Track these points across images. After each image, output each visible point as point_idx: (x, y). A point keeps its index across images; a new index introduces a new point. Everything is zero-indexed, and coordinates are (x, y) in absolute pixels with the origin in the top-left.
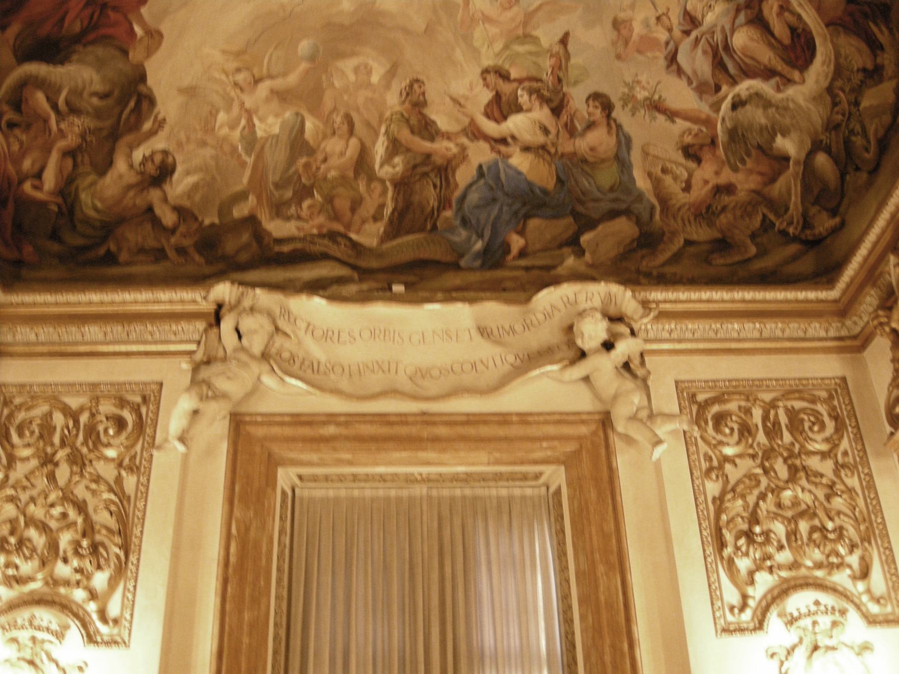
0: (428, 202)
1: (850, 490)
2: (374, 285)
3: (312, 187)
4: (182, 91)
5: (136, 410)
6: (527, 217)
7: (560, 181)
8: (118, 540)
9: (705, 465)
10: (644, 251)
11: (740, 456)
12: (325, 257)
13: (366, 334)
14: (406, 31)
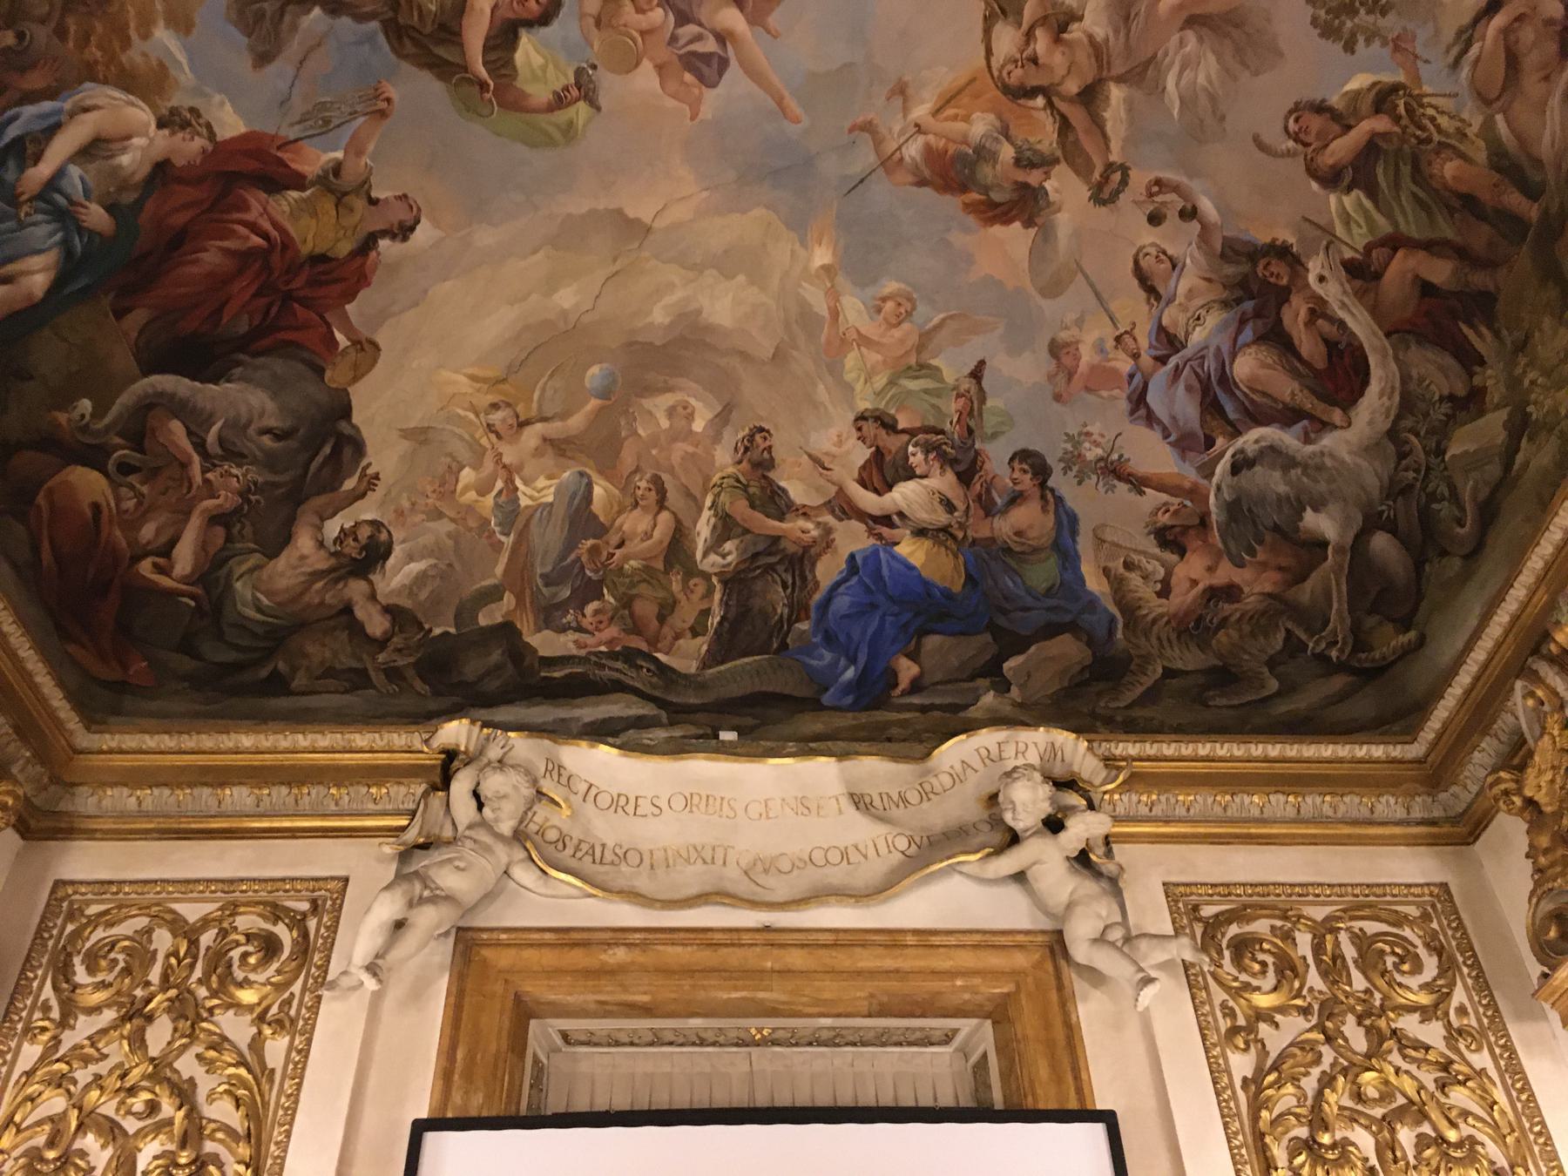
0: (775, 609)
2: (693, 730)
3: (601, 582)
4: (406, 434)
5: (298, 922)
6: (924, 632)
7: (970, 579)
8: (244, 1151)
9: (1224, 1024)
10: (1101, 686)
11: (1282, 1010)
12: (619, 687)
13: (679, 803)
14: (745, 356)
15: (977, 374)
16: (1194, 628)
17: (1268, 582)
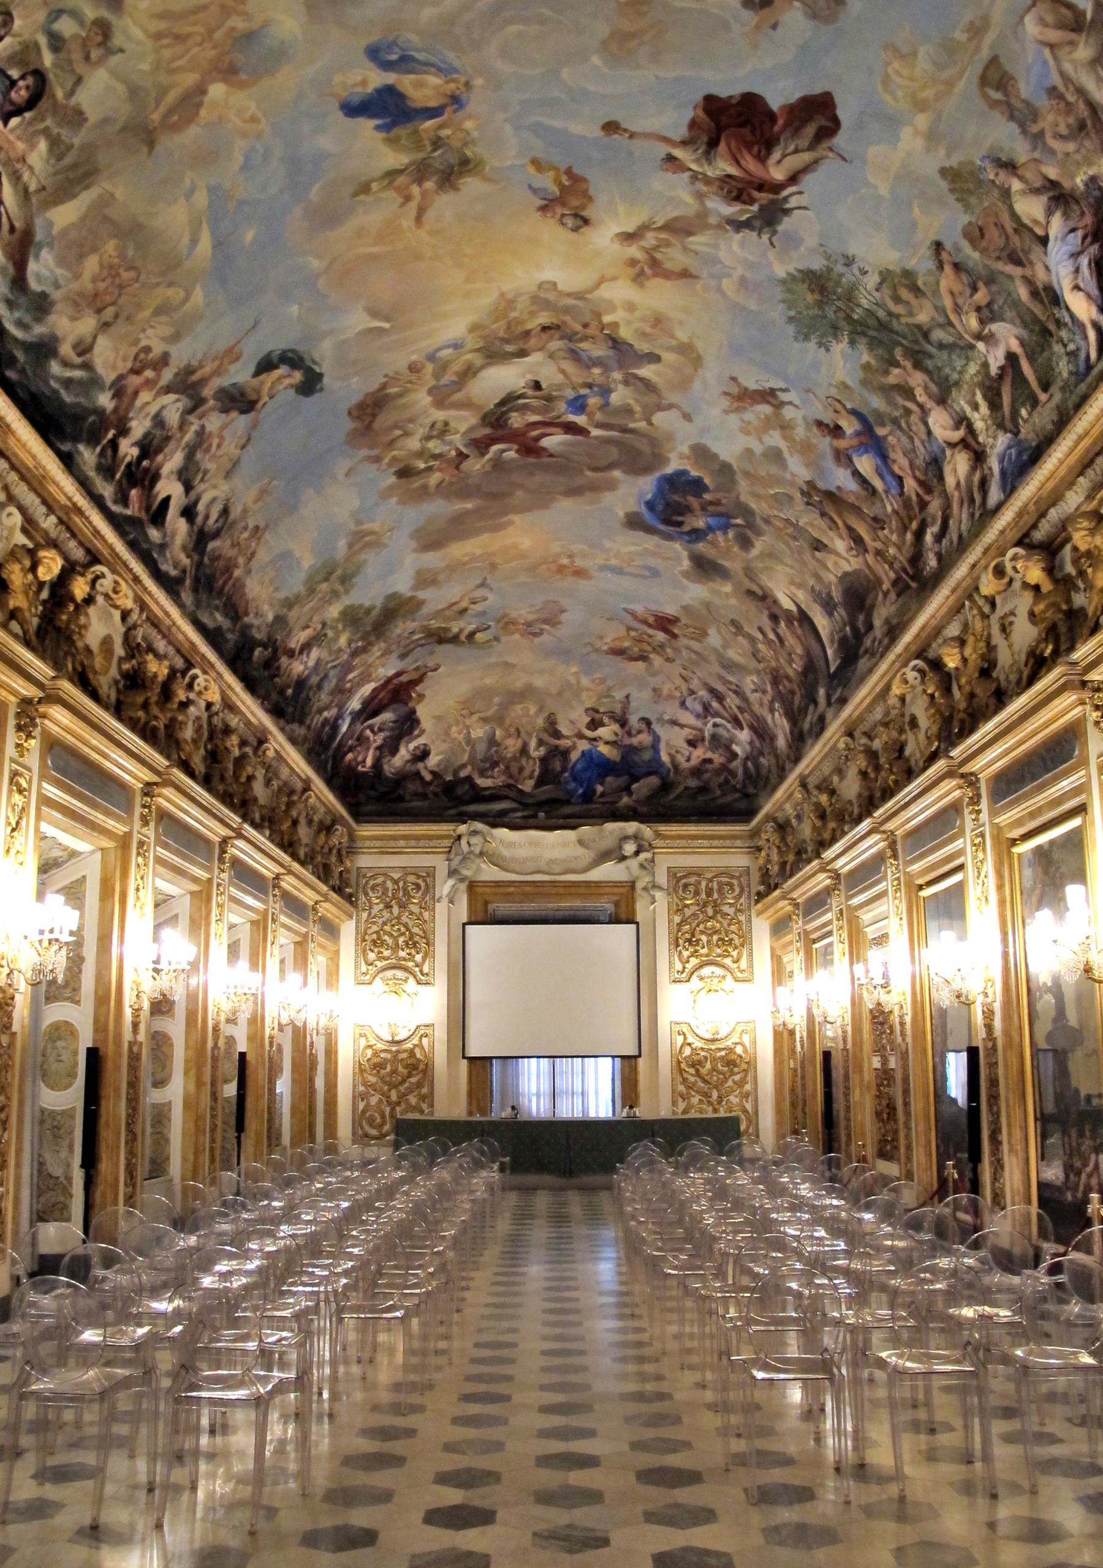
1: (739, 922)
12: (506, 798)
15: (627, 697)
16: (697, 772)
17: (722, 760)
